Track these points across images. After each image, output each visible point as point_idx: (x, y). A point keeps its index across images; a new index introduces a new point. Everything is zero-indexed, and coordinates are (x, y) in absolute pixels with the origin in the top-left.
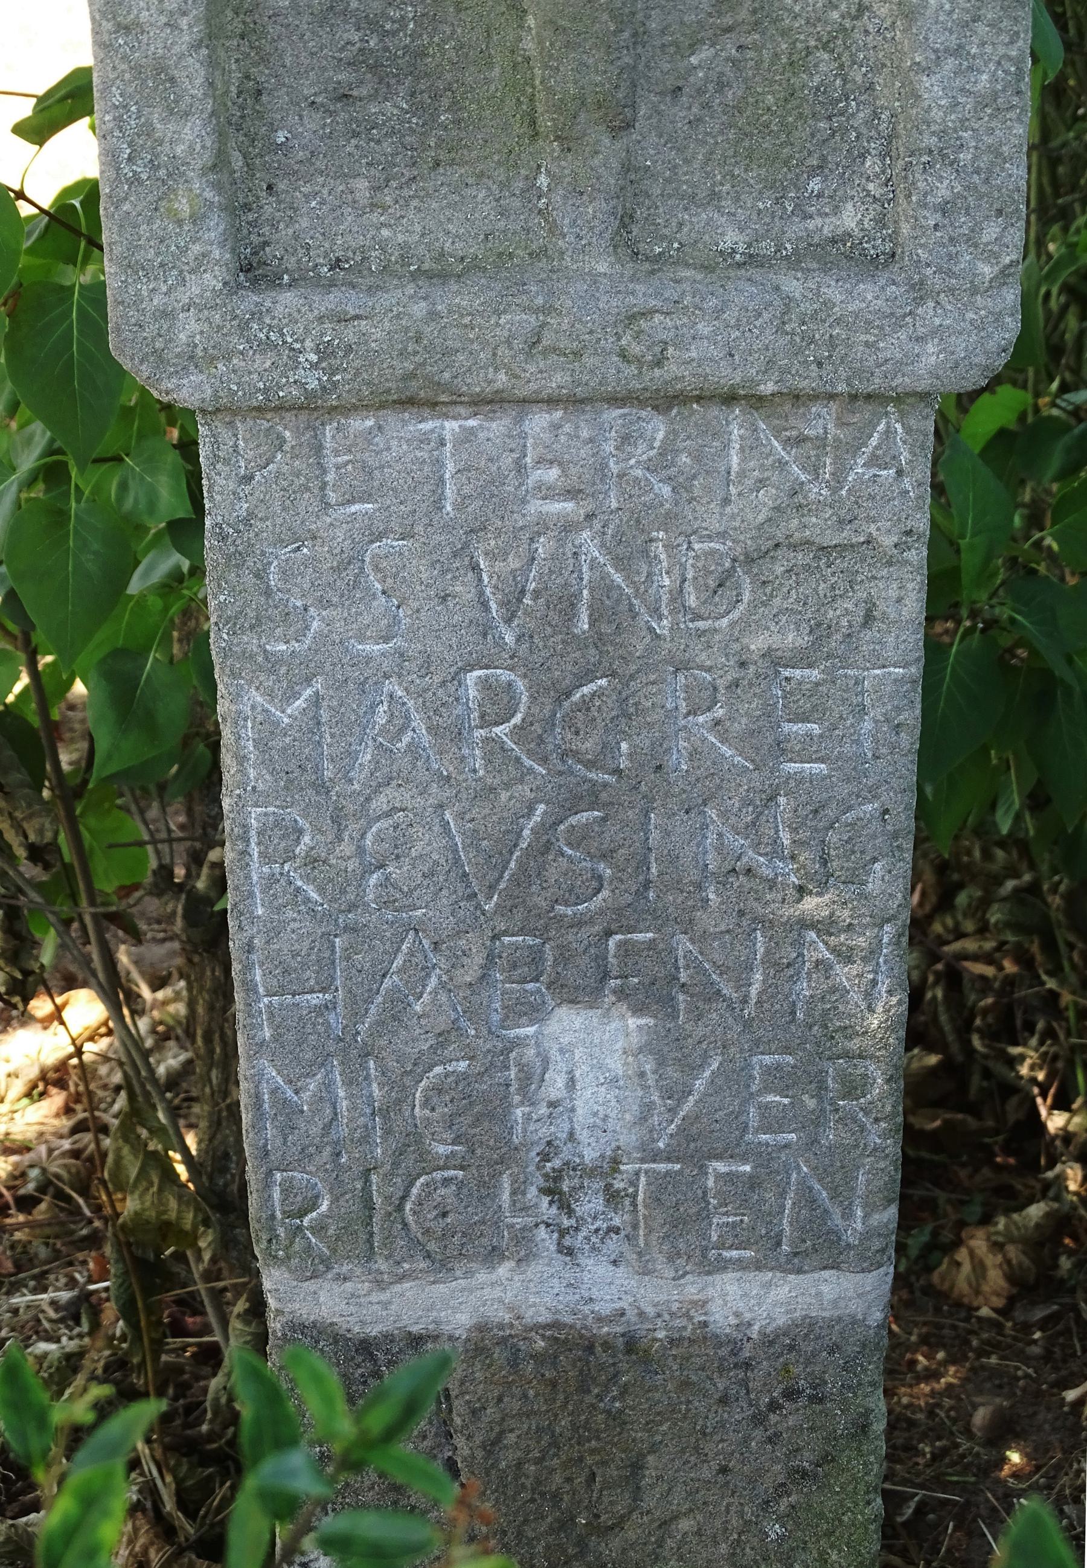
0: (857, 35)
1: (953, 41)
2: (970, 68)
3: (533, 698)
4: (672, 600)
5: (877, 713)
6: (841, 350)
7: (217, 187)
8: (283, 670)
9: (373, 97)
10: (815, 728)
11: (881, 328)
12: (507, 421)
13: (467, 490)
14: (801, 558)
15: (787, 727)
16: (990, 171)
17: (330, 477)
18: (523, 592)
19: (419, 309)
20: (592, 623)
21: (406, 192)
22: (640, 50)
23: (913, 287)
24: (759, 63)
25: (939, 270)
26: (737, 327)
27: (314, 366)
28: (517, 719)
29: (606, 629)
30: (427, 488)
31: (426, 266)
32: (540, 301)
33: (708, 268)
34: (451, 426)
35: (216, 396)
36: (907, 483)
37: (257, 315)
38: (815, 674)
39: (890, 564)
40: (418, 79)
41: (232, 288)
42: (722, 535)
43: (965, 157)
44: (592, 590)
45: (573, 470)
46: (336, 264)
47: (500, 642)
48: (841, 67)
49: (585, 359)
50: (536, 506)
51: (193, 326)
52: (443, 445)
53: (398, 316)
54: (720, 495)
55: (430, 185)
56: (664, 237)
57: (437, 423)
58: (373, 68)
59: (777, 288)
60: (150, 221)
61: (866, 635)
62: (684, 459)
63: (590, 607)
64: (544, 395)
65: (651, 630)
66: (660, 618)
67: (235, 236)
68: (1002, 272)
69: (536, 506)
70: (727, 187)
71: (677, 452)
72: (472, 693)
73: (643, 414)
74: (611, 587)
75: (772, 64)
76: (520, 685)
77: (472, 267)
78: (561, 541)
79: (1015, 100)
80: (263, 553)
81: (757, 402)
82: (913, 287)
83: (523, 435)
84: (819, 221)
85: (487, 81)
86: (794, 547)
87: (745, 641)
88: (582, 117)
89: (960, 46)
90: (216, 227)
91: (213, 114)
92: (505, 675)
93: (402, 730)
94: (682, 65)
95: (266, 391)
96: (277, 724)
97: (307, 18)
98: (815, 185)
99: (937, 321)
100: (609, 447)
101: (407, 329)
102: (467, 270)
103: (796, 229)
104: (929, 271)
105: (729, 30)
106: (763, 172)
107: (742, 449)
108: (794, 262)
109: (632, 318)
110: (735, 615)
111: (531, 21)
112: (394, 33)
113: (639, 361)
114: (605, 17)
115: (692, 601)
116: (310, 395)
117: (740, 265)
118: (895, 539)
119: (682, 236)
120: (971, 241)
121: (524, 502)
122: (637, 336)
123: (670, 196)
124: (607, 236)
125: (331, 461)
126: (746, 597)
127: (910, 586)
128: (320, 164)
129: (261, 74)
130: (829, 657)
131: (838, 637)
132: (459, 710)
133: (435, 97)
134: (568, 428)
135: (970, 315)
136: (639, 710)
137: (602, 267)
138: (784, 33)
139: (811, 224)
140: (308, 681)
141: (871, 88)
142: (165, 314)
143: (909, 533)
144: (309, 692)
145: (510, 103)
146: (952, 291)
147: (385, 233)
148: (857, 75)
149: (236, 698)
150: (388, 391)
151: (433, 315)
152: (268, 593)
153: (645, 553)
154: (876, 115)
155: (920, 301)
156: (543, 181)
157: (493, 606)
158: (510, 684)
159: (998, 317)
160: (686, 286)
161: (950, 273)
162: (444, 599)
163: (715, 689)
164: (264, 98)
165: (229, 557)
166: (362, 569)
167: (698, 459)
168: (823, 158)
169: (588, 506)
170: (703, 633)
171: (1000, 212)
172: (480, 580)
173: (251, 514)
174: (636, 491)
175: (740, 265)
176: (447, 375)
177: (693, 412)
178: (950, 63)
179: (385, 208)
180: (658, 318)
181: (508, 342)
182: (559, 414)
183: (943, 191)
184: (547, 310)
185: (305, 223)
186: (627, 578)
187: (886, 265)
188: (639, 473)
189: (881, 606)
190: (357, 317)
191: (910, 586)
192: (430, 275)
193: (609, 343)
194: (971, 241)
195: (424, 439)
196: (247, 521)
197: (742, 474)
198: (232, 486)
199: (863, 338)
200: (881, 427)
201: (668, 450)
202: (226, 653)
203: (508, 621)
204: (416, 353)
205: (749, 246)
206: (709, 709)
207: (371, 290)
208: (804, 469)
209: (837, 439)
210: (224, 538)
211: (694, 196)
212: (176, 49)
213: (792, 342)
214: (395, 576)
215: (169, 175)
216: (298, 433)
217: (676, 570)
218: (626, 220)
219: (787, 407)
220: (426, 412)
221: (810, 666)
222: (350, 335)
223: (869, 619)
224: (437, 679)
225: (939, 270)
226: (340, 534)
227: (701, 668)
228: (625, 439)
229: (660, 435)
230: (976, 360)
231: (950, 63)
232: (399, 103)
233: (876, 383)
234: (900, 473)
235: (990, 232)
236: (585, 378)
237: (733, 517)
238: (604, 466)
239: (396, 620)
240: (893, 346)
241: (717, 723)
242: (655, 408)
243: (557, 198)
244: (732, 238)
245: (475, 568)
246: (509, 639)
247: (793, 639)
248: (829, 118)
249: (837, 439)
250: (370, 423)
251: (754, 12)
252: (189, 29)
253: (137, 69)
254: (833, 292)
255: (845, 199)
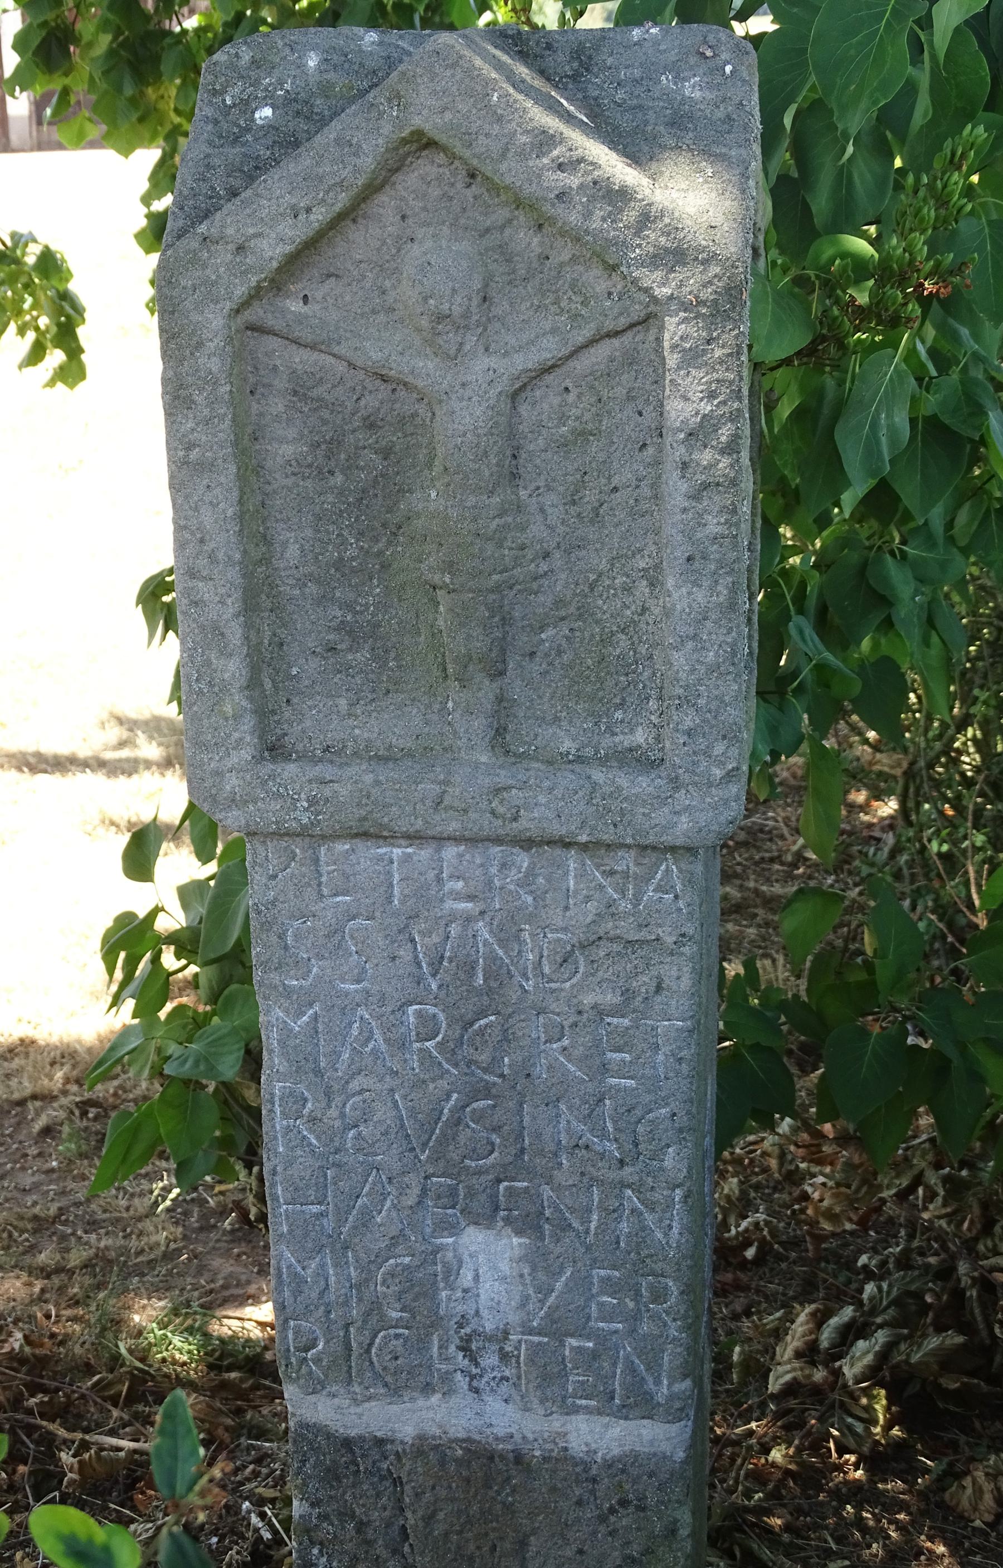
0: (643, 625)
1: (691, 631)
2: (703, 648)
3: (449, 1026)
4: (535, 969)
5: (665, 1049)
6: (628, 817)
7: (251, 699)
8: (295, 997)
9: (350, 649)
10: (627, 1057)
11: (652, 804)
12: (430, 850)
13: (406, 892)
14: (616, 947)
15: (610, 1055)
16: (717, 712)
17: (324, 879)
18: (442, 957)
19: (369, 778)
20: (485, 981)
21: (369, 708)
22: (507, 628)
23: (671, 780)
24: (583, 639)
25: (687, 771)
26: (563, 799)
27: (306, 810)
28: (439, 1038)
29: (494, 984)
30: (382, 889)
31: (380, 753)
32: (442, 777)
33: (550, 763)
34: (397, 852)
35: (248, 825)
36: (681, 904)
37: (272, 777)
38: (626, 1022)
39: (672, 954)
40: (376, 640)
41: (258, 760)
42: (565, 929)
43: (702, 702)
44: (485, 959)
45: (472, 883)
46: (327, 749)
47: (428, 988)
48: (633, 644)
49: (470, 814)
50: (449, 904)
51: (235, 781)
52: (392, 862)
53: (356, 782)
54: (563, 904)
55: (383, 704)
56: (526, 743)
57: (388, 849)
58: (349, 633)
59: (589, 777)
60: (209, 717)
61: (658, 999)
62: (541, 880)
63: (484, 970)
64: (445, 835)
65: (521, 986)
66: (528, 979)
67: (262, 729)
68: (728, 774)
69: (449, 904)
70: (564, 714)
71: (536, 876)
72: (412, 1019)
73: (514, 850)
74: (496, 958)
75: (591, 640)
76: (442, 1016)
77: (410, 754)
78: (465, 928)
79: (731, 669)
80: (283, 924)
81: (584, 847)
82: (671, 780)
83: (441, 860)
84: (621, 737)
85: (417, 644)
86: (611, 940)
87: (580, 997)
88: (471, 668)
89: (695, 635)
90: (248, 722)
91: (247, 655)
92: (431, 1010)
93: (368, 1040)
94: (536, 639)
95: (277, 823)
96: (291, 1030)
97: (310, 601)
98: (619, 715)
99: (687, 802)
100: (494, 870)
101: (361, 791)
102: (403, 756)
103: (607, 741)
104: (681, 771)
105: (563, 619)
106: (586, 705)
107: (576, 876)
108: (603, 762)
109: (498, 791)
110: (574, 981)
111: (441, 608)
112: (362, 613)
113: (503, 817)
114: (483, 608)
115: (547, 970)
116: (304, 827)
117: (570, 762)
118: (674, 939)
119: (538, 742)
120: (707, 754)
121: (442, 901)
122: (501, 802)
123: (529, 718)
124: (487, 740)
125: (324, 869)
126: (581, 970)
127: (685, 969)
128: (318, 688)
129: (283, 633)
130: (634, 1011)
131: (640, 999)
132: (403, 1030)
133: (386, 651)
134: (468, 857)
135: (708, 800)
136: (516, 1039)
137: (484, 759)
138: (597, 622)
139: (617, 739)
140: (311, 1005)
141: (651, 657)
142: (218, 773)
143: (683, 935)
144: (311, 1012)
145: (431, 657)
146: (695, 784)
147: (357, 731)
148: (643, 649)
149: (268, 1012)
150: (351, 828)
151: (377, 783)
152: (286, 948)
153: (517, 938)
154: (654, 674)
155: (676, 789)
156: (450, 704)
157: (424, 966)
158: (434, 1016)
159: (726, 802)
160: (532, 773)
161: (693, 772)
162: (394, 958)
163: (563, 1027)
164: (285, 648)
165: (262, 924)
166: (343, 937)
167: (549, 880)
168: (623, 699)
169: (481, 906)
170: (553, 991)
171: (724, 737)
172: (416, 948)
173: (276, 899)
174: (510, 899)
175: (570, 762)
176: (386, 819)
177: (545, 852)
178: (690, 645)
179: (357, 717)
180: (514, 791)
181: (422, 801)
182: (463, 847)
183: (688, 723)
184: (446, 783)
185: (308, 723)
186: (506, 953)
187: (658, 766)
188: (512, 887)
189: (667, 982)
190: (331, 781)
191: (685, 969)
192: (378, 758)
193: (484, 805)
194: (707, 754)
195: (380, 859)
196: (273, 903)
197: (576, 892)
198: (264, 880)
199: (642, 810)
200: (663, 867)
201: (531, 873)
202: (261, 984)
203: (434, 975)
204: (367, 805)
205: (578, 750)
206: (559, 1040)
207: (341, 766)
208: (615, 891)
209: (635, 873)
210: (259, 913)
211: (544, 718)
212: (225, 617)
213: (597, 810)
214: (363, 943)
215: (220, 690)
216: (303, 850)
217: (536, 950)
218: (500, 731)
219: (603, 851)
220: (381, 842)
221: (622, 1016)
222: (327, 792)
223: (659, 989)
224: (389, 1009)
225: (687, 771)
226: (330, 915)
227: (553, 1013)
228: (504, 866)
229: (526, 865)
230: (713, 828)
231: (690, 645)
232: (363, 656)
233: (651, 839)
234: (676, 897)
235: (719, 749)
236: (470, 826)
237: (571, 918)
238: (490, 882)
239: (364, 970)
240: (661, 816)
241: (565, 1049)
242: (521, 847)
243: (457, 715)
244: (567, 745)
245: (413, 940)
246: (434, 986)
247: (610, 998)
248: (627, 675)
249: (635, 873)
250: (347, 847)
251: (578, 609)
252: (233, 605)
253: (202, 628)
254: (623, 781)
255: (638, 724)
